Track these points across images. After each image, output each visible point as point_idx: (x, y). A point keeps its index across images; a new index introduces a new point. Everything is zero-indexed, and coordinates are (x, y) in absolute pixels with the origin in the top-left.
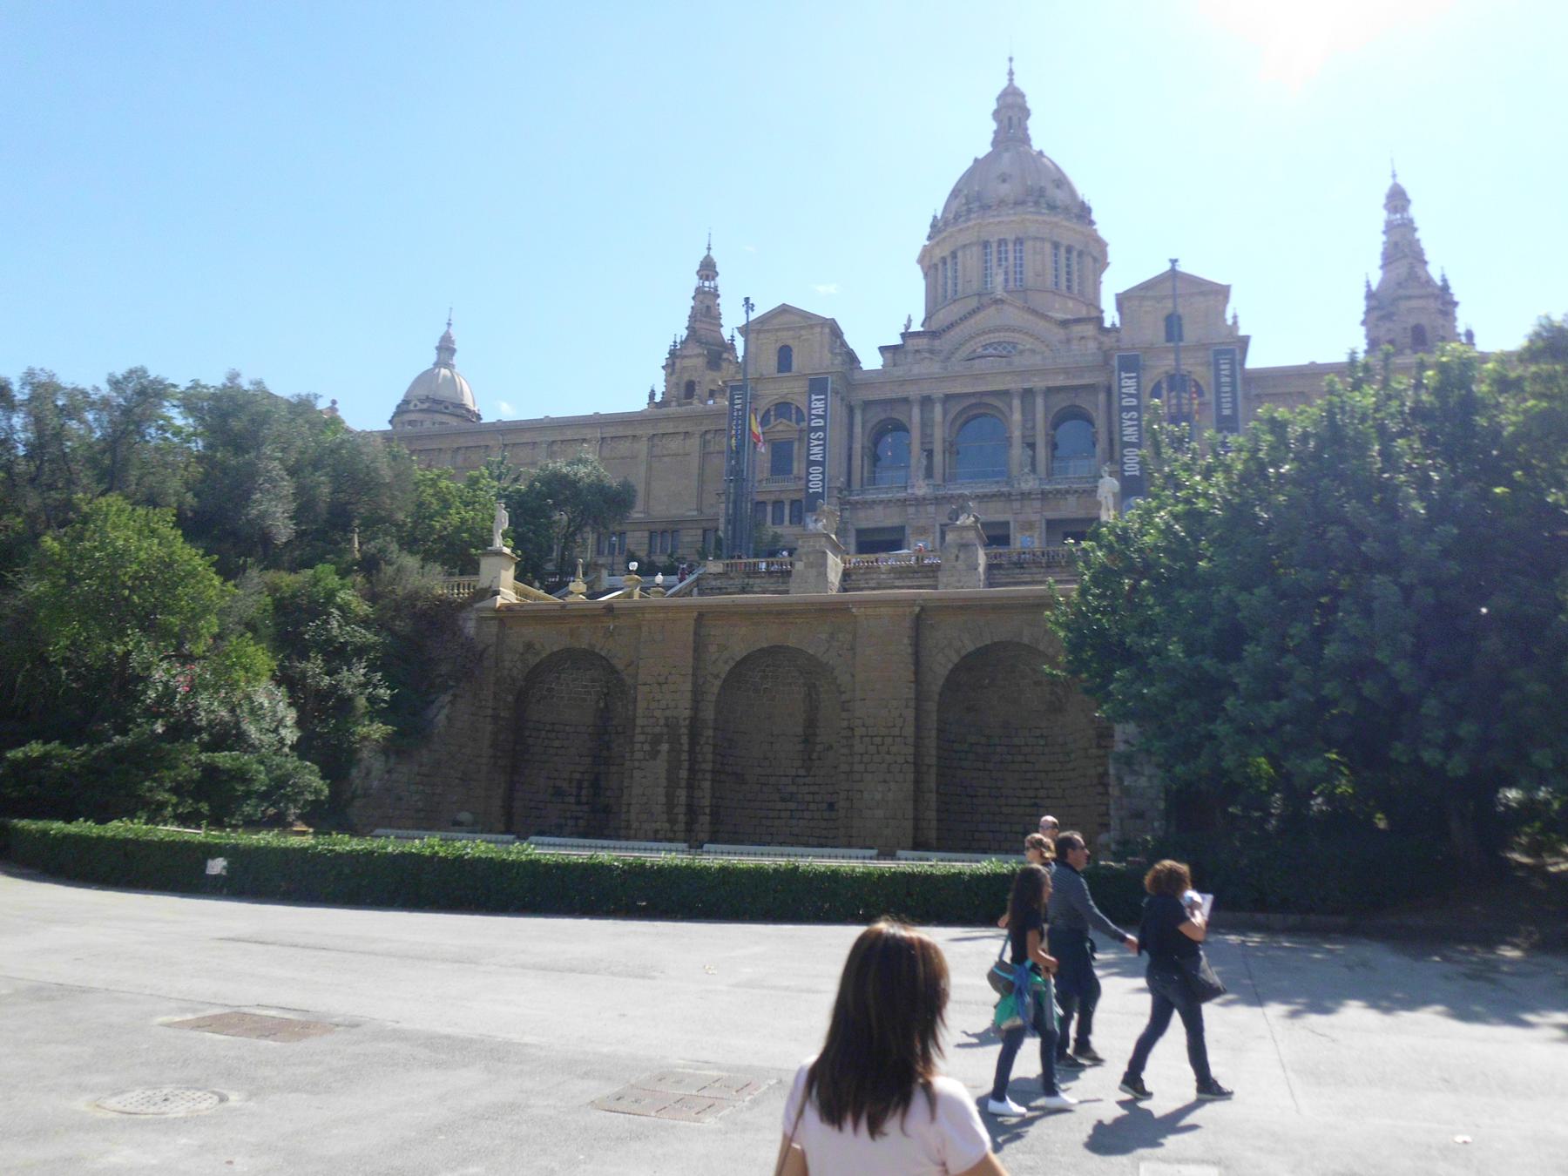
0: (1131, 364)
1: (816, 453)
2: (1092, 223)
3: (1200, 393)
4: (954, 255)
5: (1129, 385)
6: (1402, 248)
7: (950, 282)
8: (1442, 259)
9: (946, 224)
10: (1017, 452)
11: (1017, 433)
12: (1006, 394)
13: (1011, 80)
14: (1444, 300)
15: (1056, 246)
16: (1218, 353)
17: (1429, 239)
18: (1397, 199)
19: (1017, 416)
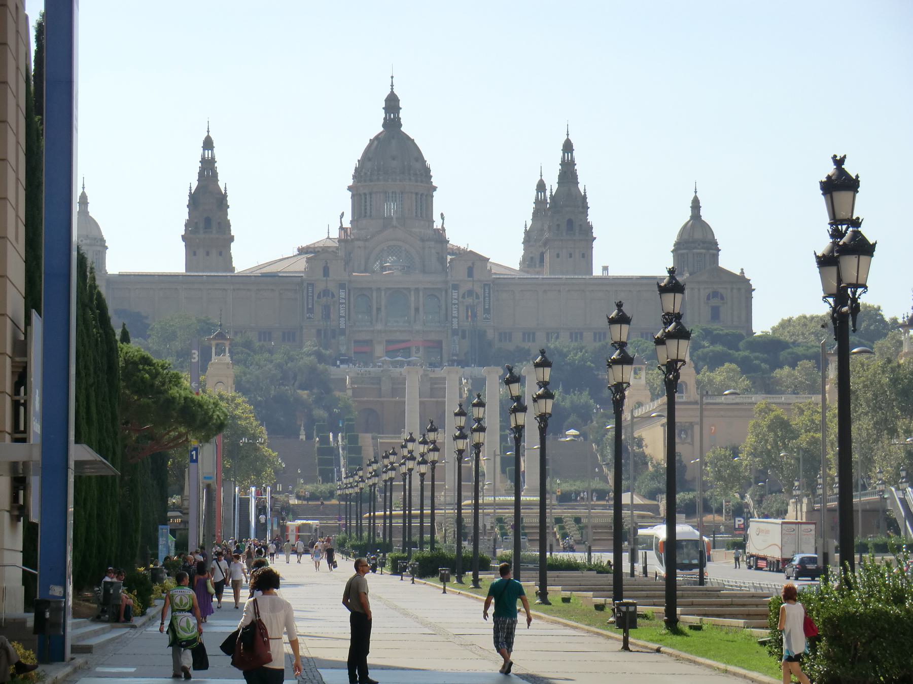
0: (456, 287)
1: (342, 313)
2: (431, 177)
3: (478, 297)
4: (371, 194)
5: (455, 295)
6: (568, 172)
7: (368, 208)
8: (585, 182)
9: (366, 174)
10: (412, 312)
11: (413, 305)
12: (409, 289)
13: (392, 89)
14: (581, 204)
15: (417, 194)
16: (485, 285)
17: (581, 169)
18: (568, 147)
19: (413, 299)
